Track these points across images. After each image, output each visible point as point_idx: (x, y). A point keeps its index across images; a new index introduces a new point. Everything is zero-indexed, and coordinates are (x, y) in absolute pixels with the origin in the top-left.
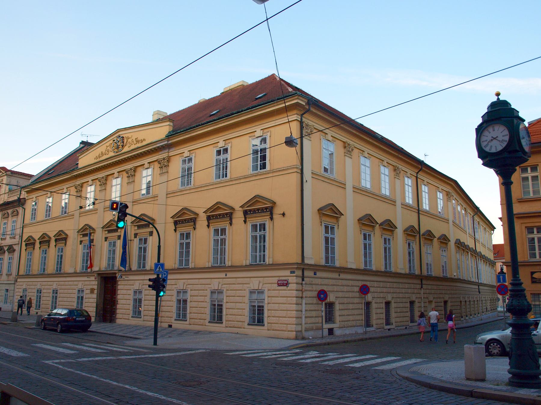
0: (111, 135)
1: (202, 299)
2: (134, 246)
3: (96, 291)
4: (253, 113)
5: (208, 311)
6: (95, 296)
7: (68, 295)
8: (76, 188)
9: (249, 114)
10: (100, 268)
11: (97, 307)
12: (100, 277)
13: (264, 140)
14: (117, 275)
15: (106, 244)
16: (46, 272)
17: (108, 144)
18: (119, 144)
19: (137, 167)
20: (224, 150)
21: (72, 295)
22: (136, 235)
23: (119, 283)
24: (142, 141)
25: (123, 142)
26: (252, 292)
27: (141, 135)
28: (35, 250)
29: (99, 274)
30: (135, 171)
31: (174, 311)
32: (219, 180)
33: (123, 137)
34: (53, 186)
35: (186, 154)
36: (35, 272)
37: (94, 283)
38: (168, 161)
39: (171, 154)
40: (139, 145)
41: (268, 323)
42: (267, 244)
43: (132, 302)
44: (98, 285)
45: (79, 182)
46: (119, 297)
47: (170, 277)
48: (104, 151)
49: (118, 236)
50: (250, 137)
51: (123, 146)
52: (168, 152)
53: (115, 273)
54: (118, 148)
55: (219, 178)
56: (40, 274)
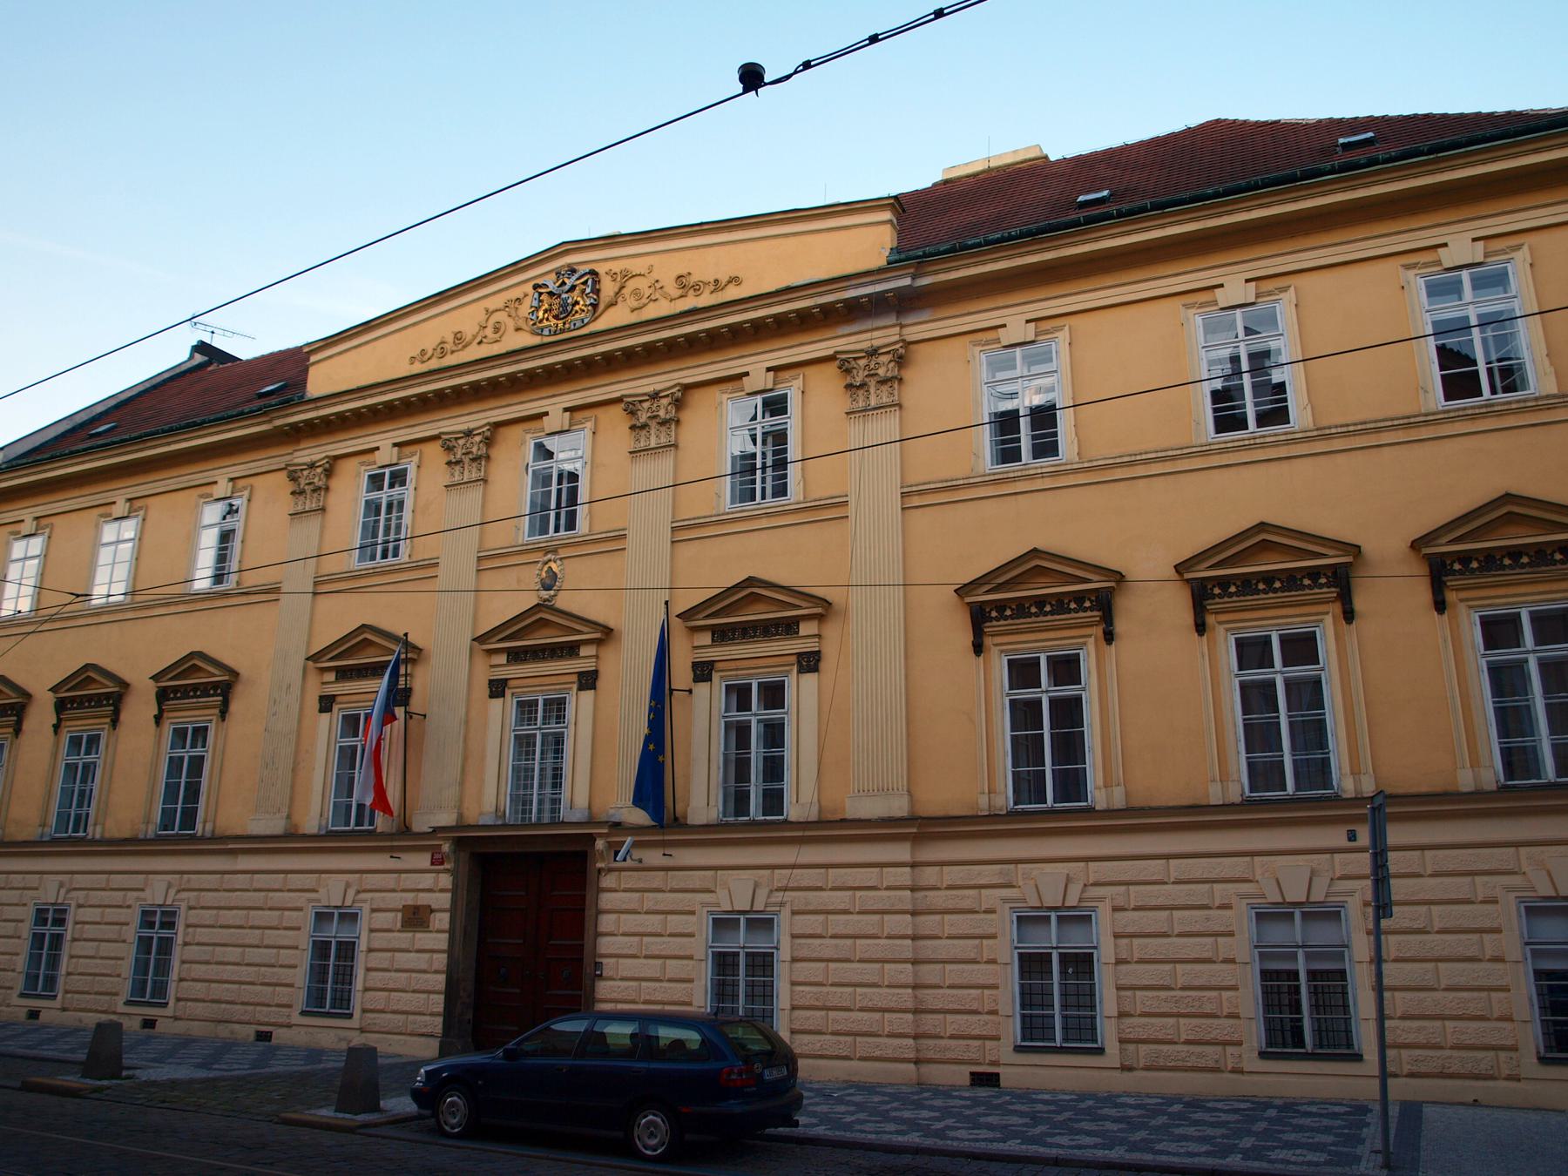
0: (516, 267)
2: (702, 717)
4: (1441, 171)
5: (300, 977)
6: (436, 938)
7: (252, 936)
8: (293, 478)
9: (1415, 176)
10: (460, 815)
11: (451, 992)
13: (776, 406)
14: (600, 844)
15: (500, 713)
16: (95, 832)
17: (497, 302)
18: (576, 295)
21: (287, 937)
22: (703, 671)
23: (608, 881)
24: (717, 286)
25: (597, 292)
27: (710, 263)
28: (25, 738)
29: (459, 843)
31: (1005, 1009)
32: (369, 564)
33: (593, 273)
35: (387, 454)
36: (30, 832)
37: (427, 880)
38: (901, 361)
40: (706, 300)
42: (789, 754)
43: (304, 959)
44: (454, 891)
45: (311, 452)
46: (605, 945)
47: (1396, 834)
48: (469, 329)
49: (580, 674)
50: (1407, 267)
51: (595, 306)
52: (902, 326)
53: (591, 838)
54: (565, 311)
55: (373, 558)
56: (54, 841)
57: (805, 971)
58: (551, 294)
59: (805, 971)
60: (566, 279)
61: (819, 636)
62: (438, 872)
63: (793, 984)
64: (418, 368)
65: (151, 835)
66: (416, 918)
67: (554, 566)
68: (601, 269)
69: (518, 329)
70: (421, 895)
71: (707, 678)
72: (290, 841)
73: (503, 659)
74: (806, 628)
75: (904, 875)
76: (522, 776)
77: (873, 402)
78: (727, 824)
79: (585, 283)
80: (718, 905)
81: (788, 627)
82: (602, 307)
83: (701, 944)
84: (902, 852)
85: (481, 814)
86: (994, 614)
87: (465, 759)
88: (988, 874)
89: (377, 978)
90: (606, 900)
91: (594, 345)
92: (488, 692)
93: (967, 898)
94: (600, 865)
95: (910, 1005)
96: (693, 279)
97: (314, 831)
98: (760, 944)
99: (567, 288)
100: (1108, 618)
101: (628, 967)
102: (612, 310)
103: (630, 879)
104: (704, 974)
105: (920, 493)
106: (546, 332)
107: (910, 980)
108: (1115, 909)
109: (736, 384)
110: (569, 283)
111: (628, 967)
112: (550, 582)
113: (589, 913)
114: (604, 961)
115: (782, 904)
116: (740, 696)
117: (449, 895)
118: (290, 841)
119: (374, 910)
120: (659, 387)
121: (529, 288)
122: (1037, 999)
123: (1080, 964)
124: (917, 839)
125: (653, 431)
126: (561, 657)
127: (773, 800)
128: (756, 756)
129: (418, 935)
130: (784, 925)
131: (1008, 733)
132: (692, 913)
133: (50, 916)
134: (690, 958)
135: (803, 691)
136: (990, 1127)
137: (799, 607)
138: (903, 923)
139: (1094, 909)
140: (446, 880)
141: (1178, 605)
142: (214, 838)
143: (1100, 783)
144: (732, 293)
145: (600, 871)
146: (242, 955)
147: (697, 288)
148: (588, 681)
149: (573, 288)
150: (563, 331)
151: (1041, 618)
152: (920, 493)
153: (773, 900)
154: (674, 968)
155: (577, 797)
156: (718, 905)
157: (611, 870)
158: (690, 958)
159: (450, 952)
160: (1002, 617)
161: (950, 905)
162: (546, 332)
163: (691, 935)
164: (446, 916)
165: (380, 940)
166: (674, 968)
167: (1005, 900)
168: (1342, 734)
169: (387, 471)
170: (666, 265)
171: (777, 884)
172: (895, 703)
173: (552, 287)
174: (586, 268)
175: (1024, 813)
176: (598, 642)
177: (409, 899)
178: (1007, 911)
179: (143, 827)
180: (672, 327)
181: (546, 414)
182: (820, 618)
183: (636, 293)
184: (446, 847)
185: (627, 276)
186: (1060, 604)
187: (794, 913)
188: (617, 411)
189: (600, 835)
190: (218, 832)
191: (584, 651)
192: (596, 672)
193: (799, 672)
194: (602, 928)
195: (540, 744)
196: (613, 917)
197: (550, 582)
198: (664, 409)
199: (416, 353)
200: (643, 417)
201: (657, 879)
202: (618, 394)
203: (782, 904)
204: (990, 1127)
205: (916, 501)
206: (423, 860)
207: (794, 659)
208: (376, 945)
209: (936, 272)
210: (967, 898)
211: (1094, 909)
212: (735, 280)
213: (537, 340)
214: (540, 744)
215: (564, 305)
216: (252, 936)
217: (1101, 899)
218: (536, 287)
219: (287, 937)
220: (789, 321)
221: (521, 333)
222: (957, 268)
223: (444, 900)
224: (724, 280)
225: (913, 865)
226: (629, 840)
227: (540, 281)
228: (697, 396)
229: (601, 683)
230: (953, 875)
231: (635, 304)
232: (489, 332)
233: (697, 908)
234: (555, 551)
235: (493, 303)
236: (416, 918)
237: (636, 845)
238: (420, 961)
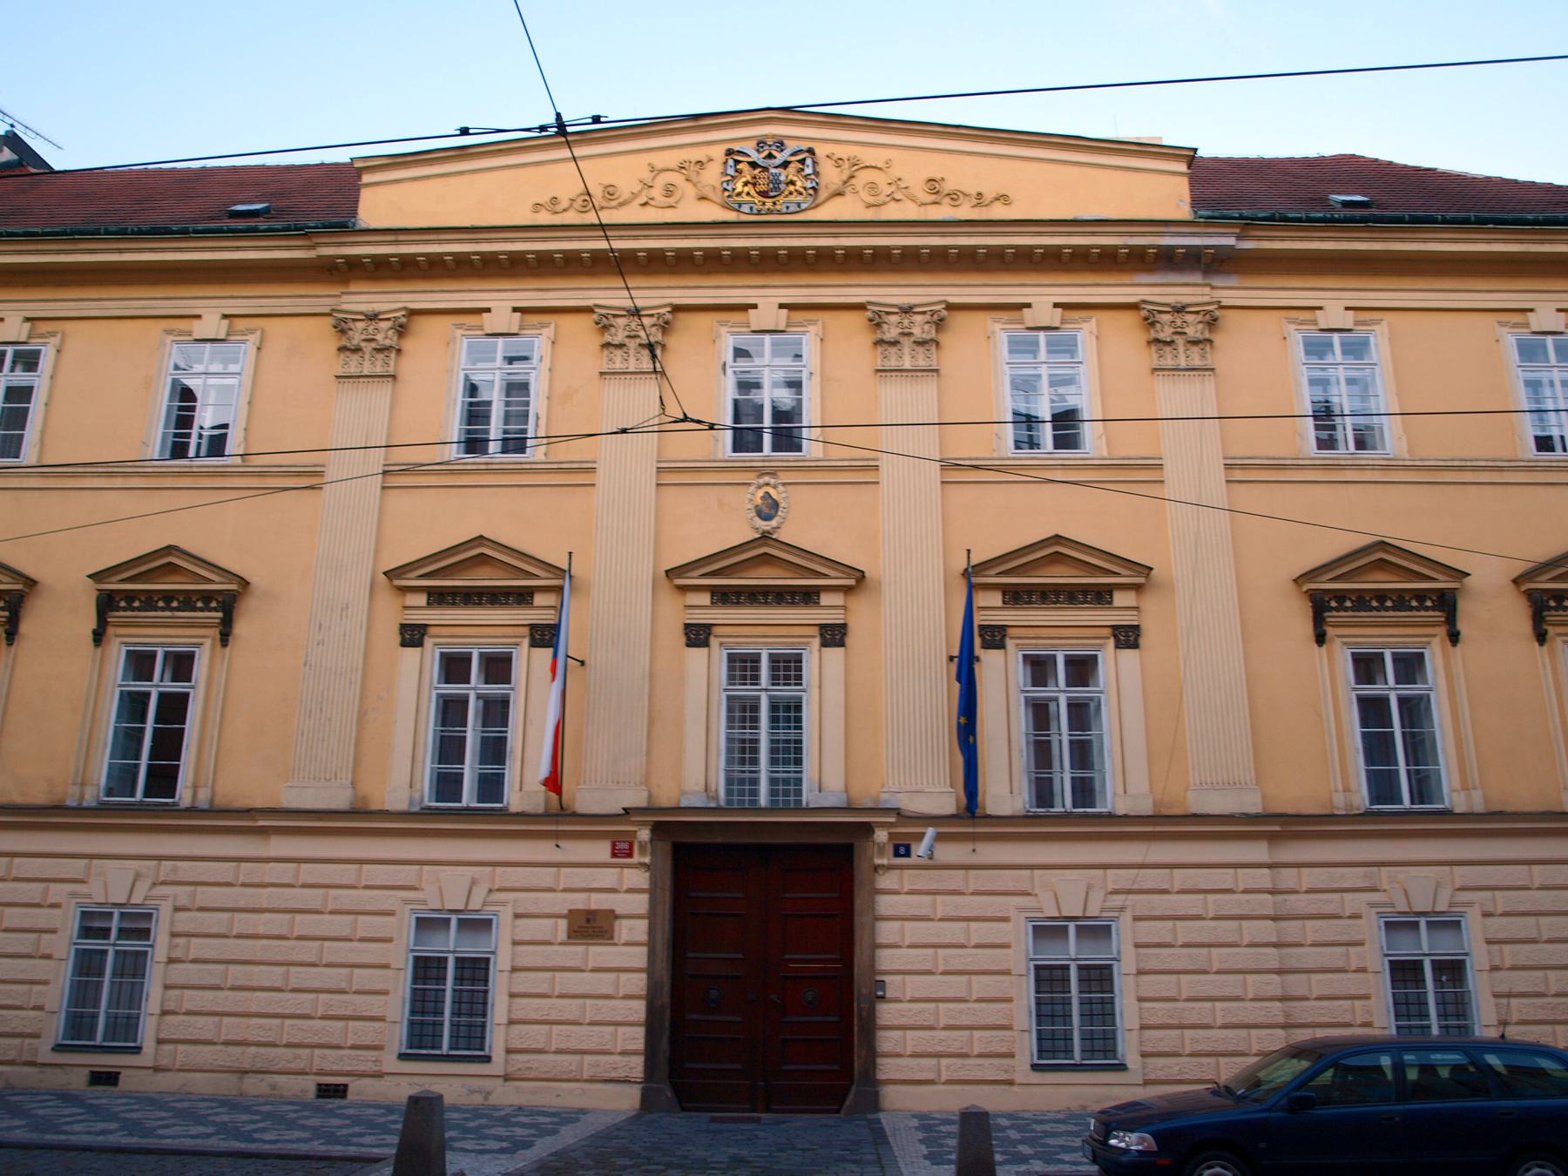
1: (373, 953)
3: (640, 929)
11: (652, 1025)
12: (665, 847)
14: (881, 836)
17: (671, 159)
19: (951, 307)
20: (18, 356)
26: (1047, 931)
29: (659, 829)
30: (402, 331)
34: (27, 285)
37: (607, 877)
39: (1229, 297)
41: (160, 1042)
48: (626, 186)
49: (822, 627)
53: (868, 829)
57: (524, 982)
58: (753, 165)
59: (524, 982)
60: (771, 149)
61: (1136, 608)
62: (622, 866)
63: (1140, 1000)
64: (544, 218)
65: (89, 800)
66: (591, 926)
67: (772, 492)
68: (821, 150)
69: (702, 198)
70: (594, 896)
71: (418, 643)
72: (358, 818)
73: (421, 600)
74: (1120, 599)
75: (1263, 878)
76: (743, 751)
77: (1183, 363)
78: (1036, 817)
79: (802, 161)
80: (1040, 910)
81: (1101, 596)
82: (823, 194)
83: (1020, 954)
84: (1258, 851)
85: (684, 793)
86: (1333, 604)
87: (651, 722)
88: (1352, 877)
89: (527, 1008)
90: (885, 904)
91: (835, 235)
92: (398, 639)
93: (1331, 903)
94: (878, 861)
95: (1281, 1020)
96: (948, 187)
97: (402, 806)
98: (1094, 955)
99: (777, 162)
100: (1451, 620)
101: (916, 986)
102: (838, 200)
103: (910, 879)
104: (1381, 989)
105: (1243, 467)
106: (746, 208)
107: (1279, 992)
108: (1486, 915)
109: (1014, 315)
110: (780, 157)
111: (916, 986)
112: (769, 509)
113: (860, 920)
114: (886, 978)
115: (1122, 909)
116: (455, 667)
117: (645, 897)
118: (358, 818)
119: (517, 916)
120: (913, 301)
121: (718, 152)
122: (1414, 1009)
123: (1452, 970)
124: (1272, 838)
125: (906, 350)
126: (793, 604)
127: (491, 786)
128: (1066, 735)
129: (594, 950)
130: (1125, 934)
131: (1357, 730)
132: (1006, 919)
133: (115, 924)
134: (1007, 973)
135: (1117, 671)
136: (500, 1139)
137: (1117, 574)
138: (1265, 930)
139: (1462, 914)
140: (641, 879)
141: (1518, 616)
142: (214, 811)
143: (1456, 784)
144: (999, 212)
145: (876, 868)
146: (278, 973)
147: (954, 196)
148: (834, 635)
149: (785, 165)
150: (770, 212)
151: (1423, 613)
152: (1243, 467)
153: (1109, 904)
154: (981, 986)
155: (826, 779)
156: (1040, 910)
157: (890, 868)
158: (1007, 973)
159: (650, 970)
160: (1341, 608)
161: (1312, 910)
162: (746, 208)
163: (1005, 946)
164: (643, 925)
165: (529, 956)
166: (981, 986)
167: (1372, 905)
168: (1452, 752)
169: (10, 350)
170: (914, 165)
171: (1110, 887)
172: (1218, 688)
173: (755, 157)
174: (805, 145)
175: (1380, 814)
176: (847, 590)
177: (579, 901)
178: (1374, 917)
179: (75, 790)
180: (943, 235)
181: (755, 306)
182: (1137, 588)
183: (872, 186)
184: (644, 834)
185: (856, 164)
186: (1401, 601)
187: (1136, 919)
188: (585, 321)
189: (882, 825)
190: (220, 802)
191: (825, 599)
192: (844, 626)
193: (1117, 647)
194: (881, 939)
195: (767, 712)
196: (896, 925)
197: (769, 509)
198: (920, 327)
199: (544, 199)
200: (891, 333)
201: (955, 879)
202: (590, 303)
203: (1122, 909)
204: (500, 1139)
205: (1238, 475)
206: (602, 851)
207: (526, 631)
208: (521, 962)
209: (1260, 238)
210: (1331, 903)
211: (1462, 914)
212: (1003, 198)
213: (731, 216)
214: (767, 712)
215: (776, 182)
216: (308, 951)
217: (1470, 904)
218: (730, 152)
219: (373, 953)
220: (498, 262)
221: (705, 205)
222: (1282, 239)
223: (641, 903)
224: (989, 196)
225: (1270, 866)
226: (930, 832)
227: (737, 147)
228: (422, 323)
229: (849, 640)
230: (1310, 878)
231: (871, 200)
232: (657, 193)
233: (1012, 913)
234: (773, 474)
235: (661, 160)
236: (591, 926)
237: (940, 837)
238: (604, 982)
